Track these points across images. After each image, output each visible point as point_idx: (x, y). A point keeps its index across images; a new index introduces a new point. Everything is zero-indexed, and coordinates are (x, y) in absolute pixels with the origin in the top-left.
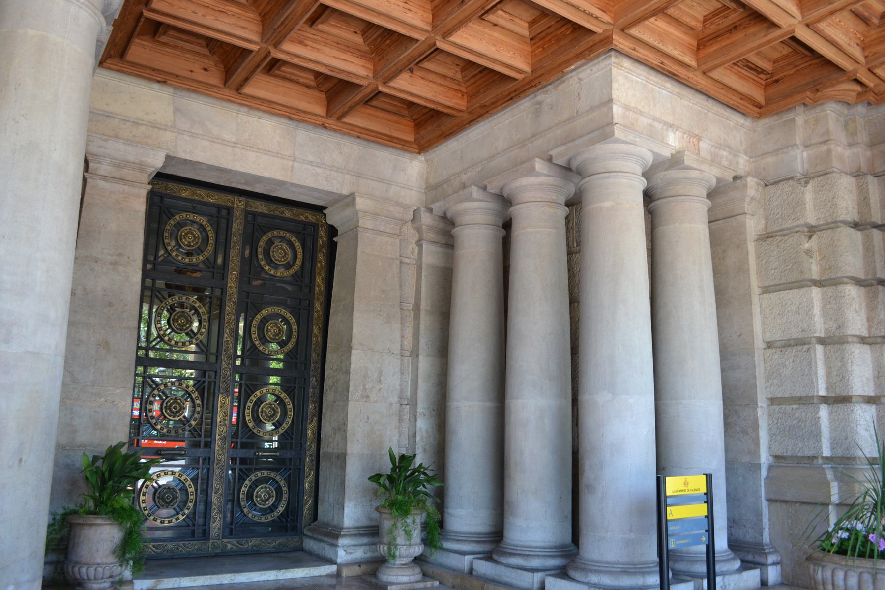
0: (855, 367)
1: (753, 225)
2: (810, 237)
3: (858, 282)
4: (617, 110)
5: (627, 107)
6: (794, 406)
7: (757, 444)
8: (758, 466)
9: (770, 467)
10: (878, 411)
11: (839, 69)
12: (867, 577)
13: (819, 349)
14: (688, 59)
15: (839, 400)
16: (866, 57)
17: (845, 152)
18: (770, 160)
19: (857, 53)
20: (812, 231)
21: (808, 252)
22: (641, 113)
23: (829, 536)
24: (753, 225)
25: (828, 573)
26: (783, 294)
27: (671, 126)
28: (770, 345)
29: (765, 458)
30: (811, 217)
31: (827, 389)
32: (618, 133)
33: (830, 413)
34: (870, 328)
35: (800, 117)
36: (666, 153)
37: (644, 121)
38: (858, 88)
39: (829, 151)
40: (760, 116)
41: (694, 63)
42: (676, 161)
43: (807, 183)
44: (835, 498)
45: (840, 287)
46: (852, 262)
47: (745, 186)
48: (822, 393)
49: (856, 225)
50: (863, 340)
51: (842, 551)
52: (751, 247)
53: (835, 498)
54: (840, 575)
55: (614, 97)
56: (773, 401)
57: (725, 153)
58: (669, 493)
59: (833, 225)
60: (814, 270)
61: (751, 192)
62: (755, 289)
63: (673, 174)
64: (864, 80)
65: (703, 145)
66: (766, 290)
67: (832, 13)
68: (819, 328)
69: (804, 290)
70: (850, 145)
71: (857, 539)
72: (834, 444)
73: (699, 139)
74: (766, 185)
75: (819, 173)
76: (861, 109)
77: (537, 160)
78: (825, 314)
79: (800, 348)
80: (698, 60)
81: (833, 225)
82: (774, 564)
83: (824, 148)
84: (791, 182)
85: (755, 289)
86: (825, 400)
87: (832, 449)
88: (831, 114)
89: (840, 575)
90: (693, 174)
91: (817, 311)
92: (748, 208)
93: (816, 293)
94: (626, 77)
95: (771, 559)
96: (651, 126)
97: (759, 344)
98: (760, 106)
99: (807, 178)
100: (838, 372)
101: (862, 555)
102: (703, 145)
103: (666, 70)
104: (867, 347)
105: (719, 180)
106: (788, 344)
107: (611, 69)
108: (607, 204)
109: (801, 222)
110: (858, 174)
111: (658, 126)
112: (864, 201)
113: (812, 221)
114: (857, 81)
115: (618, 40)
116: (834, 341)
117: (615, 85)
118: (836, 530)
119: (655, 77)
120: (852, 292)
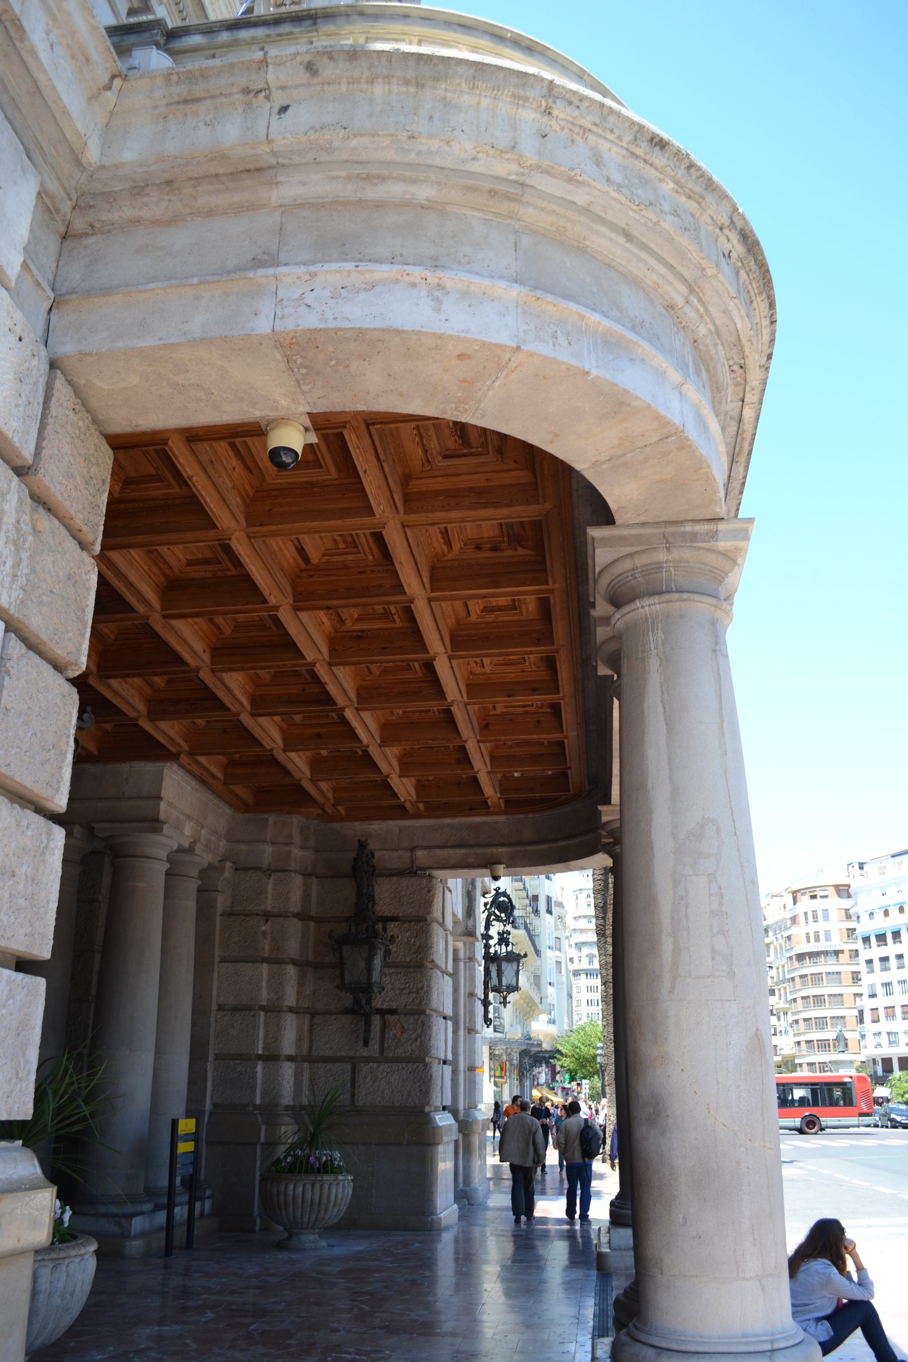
0: (286, 1032)
1: (222, 901)
2: (267, 921)
3: (294, 962)
4: (163, 805)
5: (169, 804)
6: (237, 1062)
7: (205, 1094)
8: (204, 1112)
9: (211, 1114)
10: (296, 1068)
11: (313, 801)
12: (309, 1186)
13: (262, 1014)
14: (220, 775)
15: (272, 1058)
16: (334, 798)
17: (298, 855)
18: (243, 847)
19: (330, 795)
20: (267, 916)
21: (264, 933)
22: (175, 808)
23: (279, 1161)
24: (222, 901)
25: (282, 1187)
26: (239, 965)
27: (189, 817)
28: (220, 1008)
29: (208, 1106)
30: (269, 904)
31: (264, 1048)
32: (166, 829)
33: (264, 1069)
34: (298, 1000)
35: (272, 819)
36: (186, 845)
37: (175, 814)
38: (321, 812)
39: (290, 852)
40: (246, 811)
41: (222, 778)
42: (190, 850)
43: (270, 875)
44: (262, 1140)
45: (283, 966)
46: (293, 948)
47: (223, 868)
48: (260, 1052)
49: (297, 915)
50: (291, 1010)
51: (291, 1171)
52: (218, 920)
53: (262, 1140)
54: (291, 1186)
55: (162, 795)
56: (218, 1057)
57: (214, 838)
58: (179, 1133)
59: (283, 915)
60: (266, 949)
61: (226, 874)
62: (217, 959)
63: (181, 857)
64: (328, 809)
65: (203, 832)
66: (223, 960)
67: (329, 779)
68: (264, 997)
69: (257, 965)
70: (303, 848)
71: (301, 1162)
72: (264, 1094)
73: (202, 828)
74: (236, 869)
75: (278, 869)
76: (315, 822)
77: (77, 826)
78: (269, 986)
79: (247, 1013)
80: (225, 775)
81: (283, 915)
82: (209, 1197)
83: (286, 848)
84: (258, 872)
85: (217, 959)
86: (259, 1057)
87: (262, 1098)
88: (296, 820)
89: (291, 1186)
90: (197, 859)
91: (264, 984)
92: (220, 886)
93: (265, 967)
94: (170, 777)
95: (208, 1193)
96: (178, 818)
97: (214, 1006)
98: (245, 804)
99: (270, 871)
100: (274, 1037)
101: (306, 1172)
102: (203, 832)
103: (203, 779)
104: (294, 1015)
105: (209, 863)
106: (235, 1009)
107: (163, 770)
108: (142, 885)
109: (262, 907)
110: (306, 874)
111: (182, 817)
112: (306, 897)
113: (269, 908)
114: (323, 809)
115: (184, 759)
116: (274, 1009)
117: (164, 784)
118: (285, 1157)
119: (188, 778)
120: (291, 970)
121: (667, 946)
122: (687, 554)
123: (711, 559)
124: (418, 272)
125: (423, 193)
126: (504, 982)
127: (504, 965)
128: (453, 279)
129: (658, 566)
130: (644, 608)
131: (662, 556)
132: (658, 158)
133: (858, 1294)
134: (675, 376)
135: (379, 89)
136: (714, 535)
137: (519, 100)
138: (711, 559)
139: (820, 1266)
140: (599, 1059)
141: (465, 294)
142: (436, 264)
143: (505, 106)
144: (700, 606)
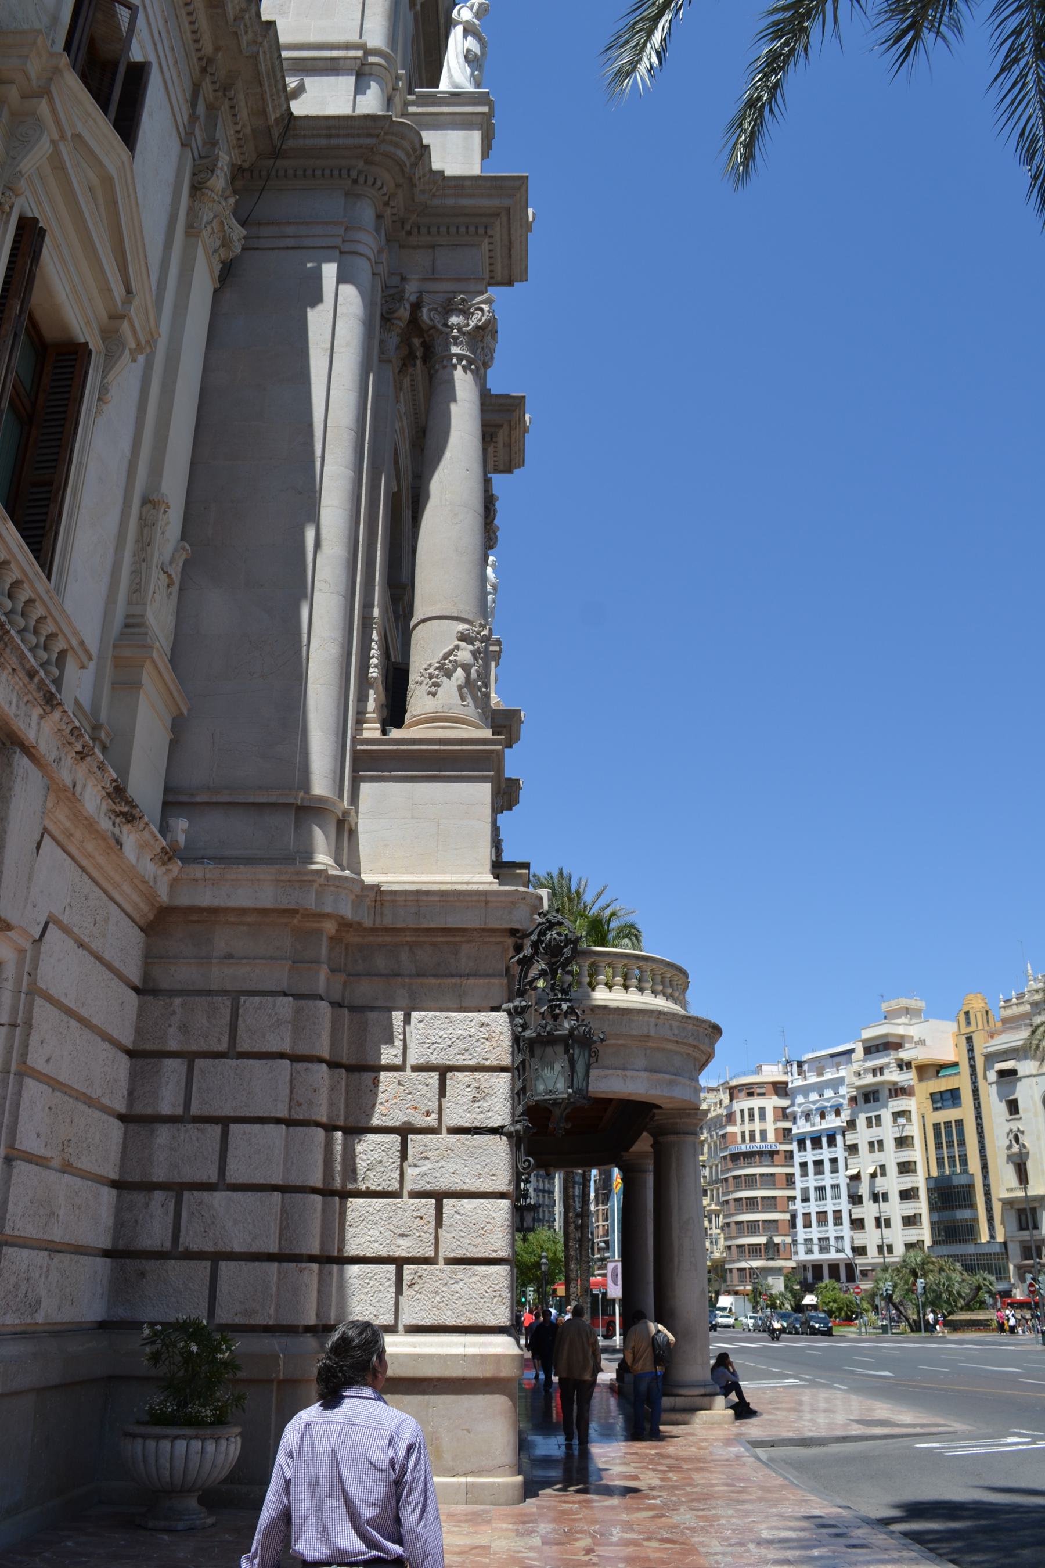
121: (676, 1260)
122: (687, 1120)
123: (695, 1121)
124: (619, 1072)
125: (621, 1042)
126: (525, 1225)
127: (525, 1213)
128: (629, 1073)
129: (677, 1123)
130: (672, 1138)
131: (678, 1121)
132: (689, 1021)
133: (733, 1378)
134: (688, 1082)
135: (611, 1016)
136: (696, 1114)
137: (650, 1017)
138: (695, 1121)
139: (722, 1369)
140: (543, 1268)
141: (632, 1077)
142: (624, 1069)
143: (646, 1019)
144: (690, 1139)
